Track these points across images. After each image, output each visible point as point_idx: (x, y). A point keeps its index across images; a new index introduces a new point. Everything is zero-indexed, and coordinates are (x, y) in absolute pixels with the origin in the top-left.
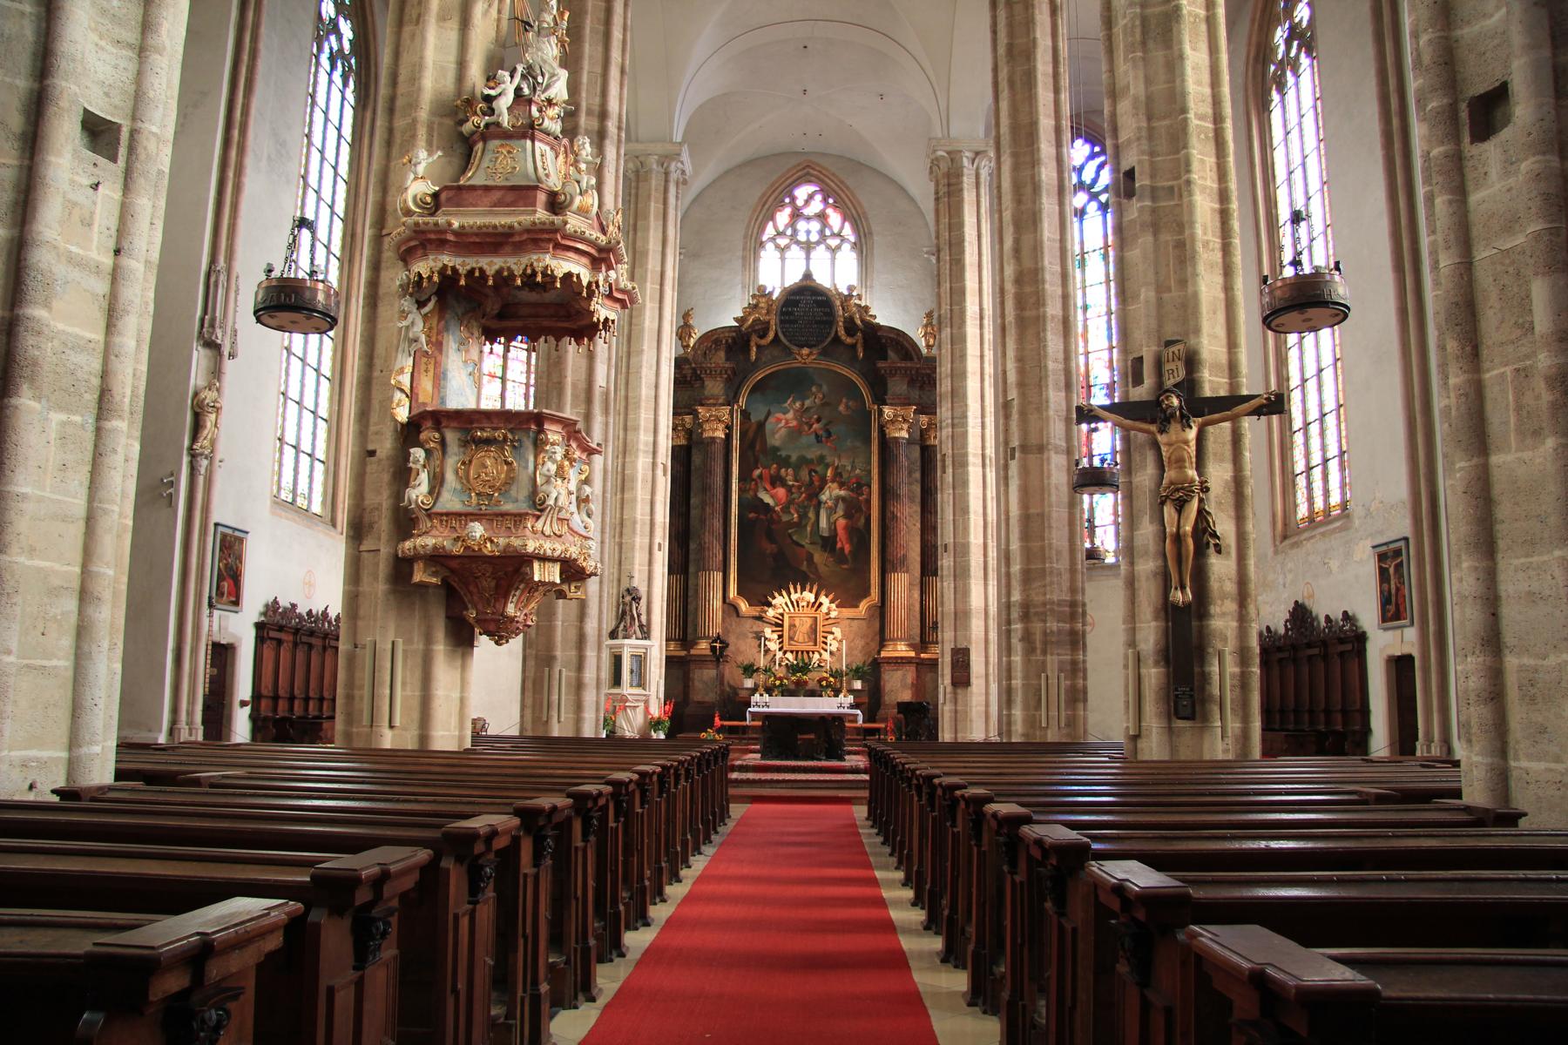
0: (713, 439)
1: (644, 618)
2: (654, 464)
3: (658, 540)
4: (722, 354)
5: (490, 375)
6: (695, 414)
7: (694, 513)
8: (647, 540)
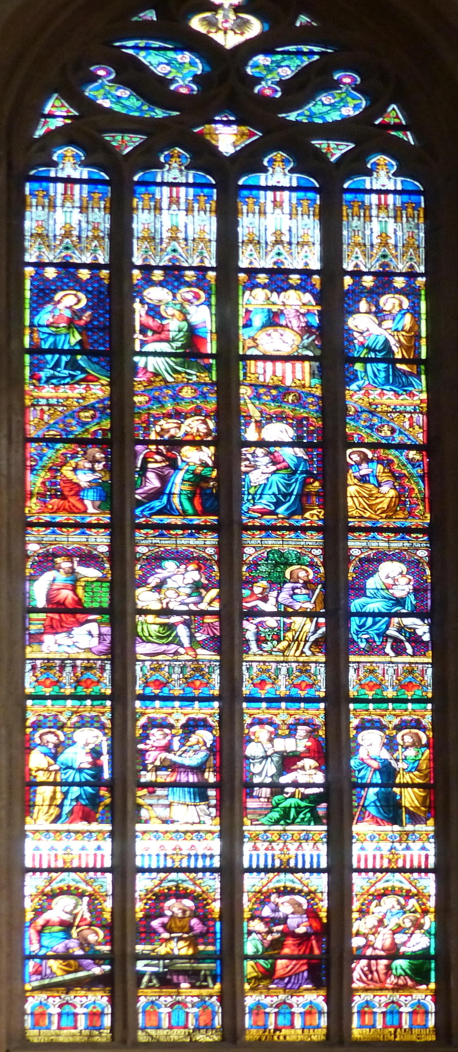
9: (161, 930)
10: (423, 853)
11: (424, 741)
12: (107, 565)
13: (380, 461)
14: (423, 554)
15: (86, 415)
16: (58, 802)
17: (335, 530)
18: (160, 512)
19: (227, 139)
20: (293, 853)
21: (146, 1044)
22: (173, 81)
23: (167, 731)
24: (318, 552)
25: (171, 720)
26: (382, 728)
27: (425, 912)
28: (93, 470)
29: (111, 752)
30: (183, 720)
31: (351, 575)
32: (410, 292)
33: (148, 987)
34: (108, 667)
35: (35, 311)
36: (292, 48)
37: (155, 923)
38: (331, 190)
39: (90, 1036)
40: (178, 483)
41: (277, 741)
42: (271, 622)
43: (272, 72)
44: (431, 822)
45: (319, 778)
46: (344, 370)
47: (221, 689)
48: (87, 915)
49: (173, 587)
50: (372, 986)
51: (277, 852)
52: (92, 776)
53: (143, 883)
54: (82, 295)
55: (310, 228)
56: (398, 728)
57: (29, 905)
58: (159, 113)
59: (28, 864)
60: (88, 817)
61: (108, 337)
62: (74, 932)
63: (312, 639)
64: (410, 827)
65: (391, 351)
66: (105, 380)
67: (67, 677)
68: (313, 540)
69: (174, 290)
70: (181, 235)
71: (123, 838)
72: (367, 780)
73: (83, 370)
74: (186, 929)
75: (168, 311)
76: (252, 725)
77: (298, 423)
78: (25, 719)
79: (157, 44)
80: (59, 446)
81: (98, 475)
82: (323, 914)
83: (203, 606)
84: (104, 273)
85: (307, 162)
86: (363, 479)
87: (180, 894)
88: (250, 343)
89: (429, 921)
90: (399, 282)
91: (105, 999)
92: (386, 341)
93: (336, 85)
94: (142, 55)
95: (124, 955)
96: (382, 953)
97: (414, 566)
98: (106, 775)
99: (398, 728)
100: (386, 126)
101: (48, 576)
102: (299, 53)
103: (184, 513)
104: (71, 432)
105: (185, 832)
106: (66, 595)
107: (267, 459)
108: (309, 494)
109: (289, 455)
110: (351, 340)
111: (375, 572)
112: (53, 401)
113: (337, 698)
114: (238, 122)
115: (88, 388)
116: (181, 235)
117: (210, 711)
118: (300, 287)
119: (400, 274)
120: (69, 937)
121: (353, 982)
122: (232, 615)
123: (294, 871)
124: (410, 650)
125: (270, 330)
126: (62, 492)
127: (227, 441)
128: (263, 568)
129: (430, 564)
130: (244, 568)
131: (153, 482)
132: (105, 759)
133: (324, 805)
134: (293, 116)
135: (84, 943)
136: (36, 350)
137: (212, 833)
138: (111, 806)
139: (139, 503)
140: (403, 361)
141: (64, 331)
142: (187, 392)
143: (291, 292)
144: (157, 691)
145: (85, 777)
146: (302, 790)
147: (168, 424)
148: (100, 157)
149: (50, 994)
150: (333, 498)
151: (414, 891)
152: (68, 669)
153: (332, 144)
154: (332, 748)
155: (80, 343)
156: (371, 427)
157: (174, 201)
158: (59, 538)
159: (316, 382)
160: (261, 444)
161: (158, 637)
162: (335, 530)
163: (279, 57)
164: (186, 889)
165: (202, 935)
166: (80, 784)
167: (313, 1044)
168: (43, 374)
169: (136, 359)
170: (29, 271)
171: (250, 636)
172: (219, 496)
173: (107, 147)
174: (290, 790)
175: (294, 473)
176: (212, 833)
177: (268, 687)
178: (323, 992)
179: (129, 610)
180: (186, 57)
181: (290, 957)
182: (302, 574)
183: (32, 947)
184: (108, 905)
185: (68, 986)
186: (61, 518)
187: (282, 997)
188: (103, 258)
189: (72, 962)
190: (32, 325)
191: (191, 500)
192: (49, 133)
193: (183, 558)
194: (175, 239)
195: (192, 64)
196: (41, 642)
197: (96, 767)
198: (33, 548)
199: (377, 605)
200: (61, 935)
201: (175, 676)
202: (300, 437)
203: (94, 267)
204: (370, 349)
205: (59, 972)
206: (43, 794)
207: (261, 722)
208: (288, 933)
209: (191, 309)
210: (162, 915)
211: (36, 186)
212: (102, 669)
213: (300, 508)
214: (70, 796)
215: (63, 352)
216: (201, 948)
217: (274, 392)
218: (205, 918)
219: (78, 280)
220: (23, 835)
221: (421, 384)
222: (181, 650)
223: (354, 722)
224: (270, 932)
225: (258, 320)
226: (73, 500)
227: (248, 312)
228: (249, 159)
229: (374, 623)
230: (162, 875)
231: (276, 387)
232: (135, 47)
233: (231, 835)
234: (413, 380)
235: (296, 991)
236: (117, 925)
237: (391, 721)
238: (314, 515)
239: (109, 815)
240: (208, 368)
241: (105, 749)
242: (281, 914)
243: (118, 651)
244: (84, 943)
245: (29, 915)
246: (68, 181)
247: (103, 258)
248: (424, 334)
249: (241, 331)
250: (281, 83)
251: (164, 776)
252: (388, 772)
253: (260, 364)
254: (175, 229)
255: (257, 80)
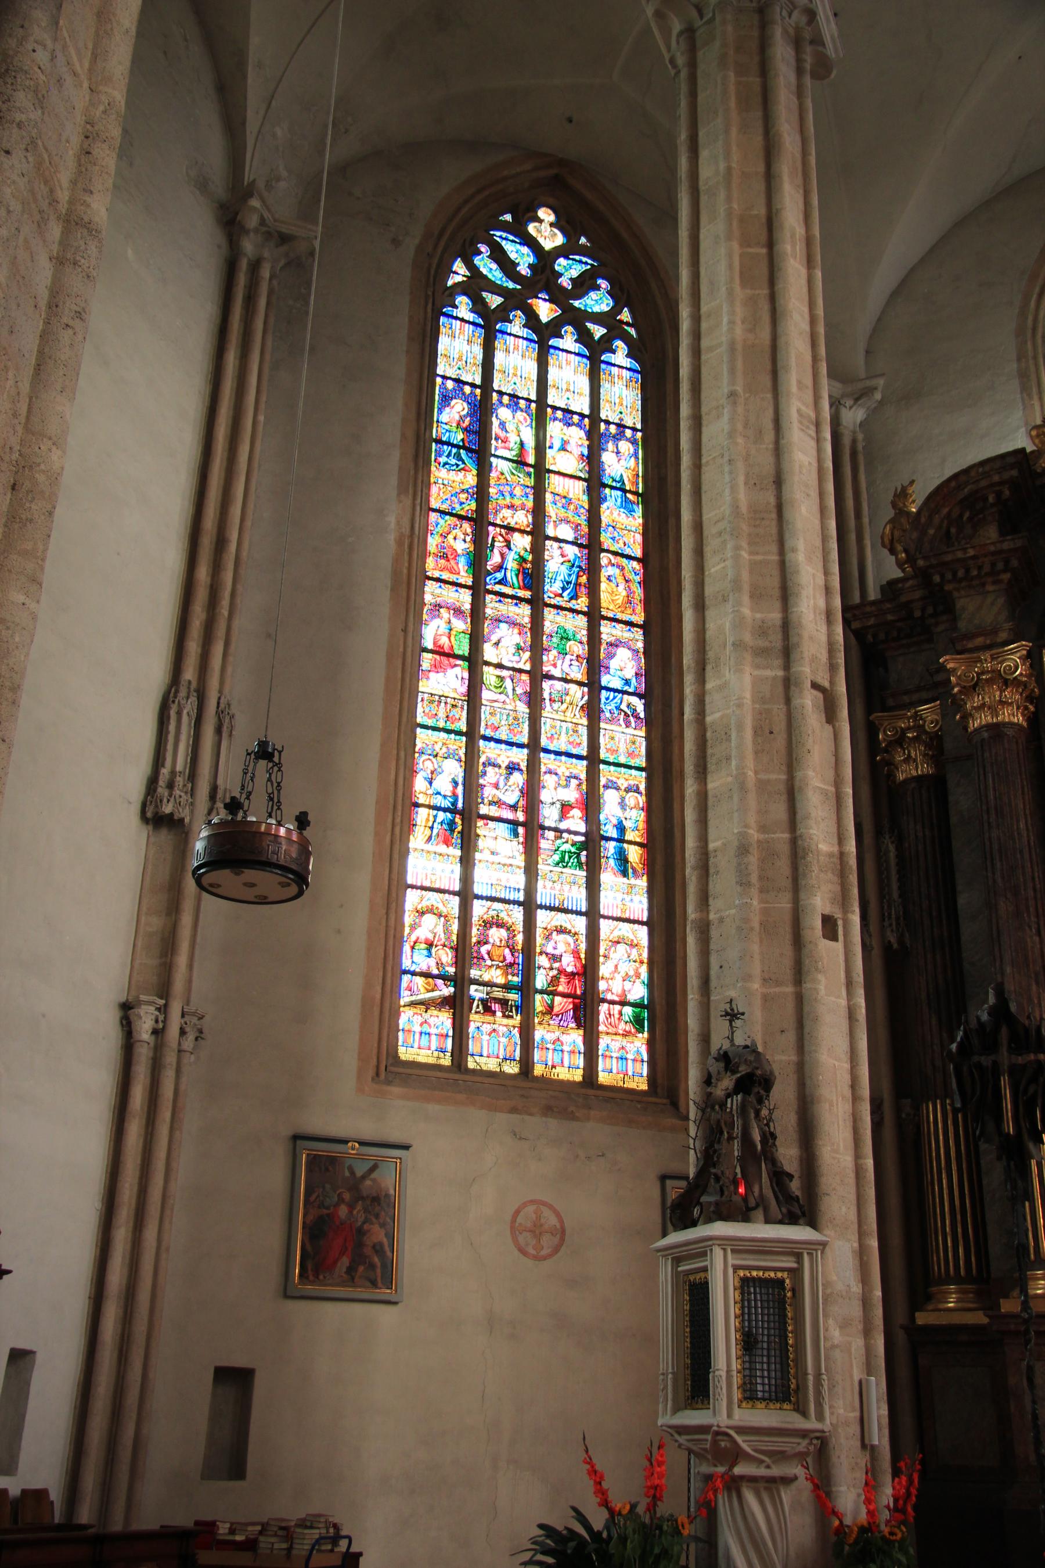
0: (996, 730)
1: (788, 1155)
2: (788, 684)
3: (820, 901)
4: (991, 533)
5: (439, 651)
6: (936, 686)
7: (969, 930)
8: (785, 904)
9: (486, 957)
10: (641, 906)
11: (641, 805)
12: (469, 620)
13: (618, 566)
14: (640, 645)
15: (463, 496)
16: (430, 824)
17: (594, 616)
18: (500, 583)
19: (545, 311)
20: (566, 894)
21: (474, 1071)
22: (518, 264)
23: (496, 769)
24: (585, 632)
25: (499, 761)
26: (618, 789)
27: (642, 962)
28: (465, 541)
29: (464, 785)
30: (506, 763)
31: (602, 655)
32: (634, 442)
33: (476, 1012)
34: (465, 707)
35: (440, 411)
36: (577, 258)
37: (484, 950)
38: (595, 354)
39: (438, 1058)
40: (511, 564)
41: (560, 789)
42: (559, 685)
43: (569, 270)
44: (645, 878)
45: (582, 827)
46: (600, 493)
47: (529, 738)
48: (442, 936)
49: (504, 645)
50: (610, 1031)
51: (557, 892)
52: (453, 805)
53: (479, 909)
54: (465, 405)
55: (583, 383)
56: (628, 790)
57: (408, 920)
58: (511, 285)
59: (409, 881)
60: (447, 842)
61: (478, 446)
62: (434, 950)
63: (580, 705)
64: (633, 881)
65: (623, 483)
66: (475, 472)
67: (442, 714)
68: (582, 621)
69: (514, 411)
70: (519, 374)
71: (467, 862)
72: (608, 835)
73: (464, 463)
74: (501, 958)
75: (510, 427)
76: (545, 773)
77: (577, 527)
78: (415, 745)
79: (511, 237)
80: (447, 517)
81: (467, 545)
82: (583, 956)
83: (521, 666)
84: (478, 391)
85: (584, 337)
86: (609, 578)
87: (500, 925)
88: (552, 461)
89: (644, 970)
90: (628, 433)
91: (450, 1021)
92: (621, 476)
93: (597, 288)
94: (503, 243)
95: (463, 978)
96: (617, 999)
97: (636, 652)
98: (460, 805)
99: (628, 790)
100: (621, 321)
101: (436, 622)
102: (581, 262)
103: (512, 587)
104: (453, 508)
105: (504, 865)
106: (444, 641)
107: (559, 552)
108: (580, 585)
109: (572, 551)
110: (604, 471)
111: (615, 655)
112: (446, 482)
113: (593, 759)
114: (550, 301)
115: (465, 476)
116: (519, 374)
117: (520, 756)
118: (579, 425)
119: (629, 428)
120: (429, 956)
121: (598, 1025)
122: (537, 676)
123: (566, 911)
124: (633, 725)
125: (563, 453)
126: (446, 555)
127: (538, 533)
128: (554, 640)
129: (644, 653)
130: (545, 637)
131: (496, 559)
132: (460, 790)
133: (584, 853)
134: (576, 304)
135: (439, 964)
136: (439, 441)
137: (519, 867)
138: (462, 833)
139: (489, 573)
140: (630, 492)
141: (455, 429)
142: (518, 491)
143: (574, 427)
144: (492, 734)
145: (446, 804)
146: (572, 837)
147: (506, 513)
148: (479, 307)
149: (415, 1010)
150: (593, 591)
151: (635, 942)
152: (443, 704)
153: (596, 327)
154: (591, 805)
155: (463, 440)
156: (613, 539)
157: (516, 348)
158: (444, 592)
159: (585, 498)
160: (556, 539)
161: (496, 687)
162: (594, 616)
163: (570, 262)
164: (502, 919)
165: (511, 965)
166: (445, 810)
167: (574, 1083)
168: (443, 459)
169: (492, 459)
170: (439, 380)
171: (546, 695)
172: (533, 575)
173: (483, 300)
174: (565, 835)
175: (573, 566)
176: (519, 867)
177: (555, 741)
178: (581, 1032)
179: (480, 661)
180: (525, 250)
181: (564, 995)
182: (575, 649)
183: (406, 964)
184: (455, 927)
185: (426, 1004)
186: (445, 576)
187: (557, 1034)
188: (478, 382)
189: (430, 980)
190: (438, 421)
191: (517, 576)
192: (455, 285)
193: (513, 624)
194: (516, 375)
195: (528, 255)
196: (428, 678)
197: (455, 795)
198: (428, 598)
199: (617, 684)
200: (425, 952)
201: (503, 723)
202: (576, 538)
203: (473, 385)
204: (614, 480)
205: (423, 990)
206: (422, 815)
207: (550, 772)
208: (561, 971)
209: (522, 428)
210: (487, 943)
211: (446, 319)
212: (462, 708)
213: (575, 597)
214: (439, 820)
215: (453, 446)
216: (510, 977)
217: (564, 501)
218: (512, 949)
219: (464, 394)
220: (408, 852)
221: (639, 511)
222: (508, 701)
223: (603, 781)
224: (551, 969)
225: (557, 444)
226: (452, 562)
227: (551, 437)
228: (554, 329)
229: (614, 698)
230: (489, 903)
231: (565, 497)
232: (500, 237)
233: (531, 871)
234: (635, 507)
235: (565, 1029)
236: (459, 949)
237: (623, 784)
238: (582, 603)
239: (459, 841)
240: (529, 474)
241: (460, 780)
242: (557, 952)
243: (472, 695)
244: (439, 964)
245: (407, 930)
246: (462, 320)
247: (478, 382)
248: (640, 474)
249: (548, 451)
250: (571, 279)
251: (493, 811)
252: (621, 828)
253: (557, 477)
254: (515, 368)
255: (561, 275)
